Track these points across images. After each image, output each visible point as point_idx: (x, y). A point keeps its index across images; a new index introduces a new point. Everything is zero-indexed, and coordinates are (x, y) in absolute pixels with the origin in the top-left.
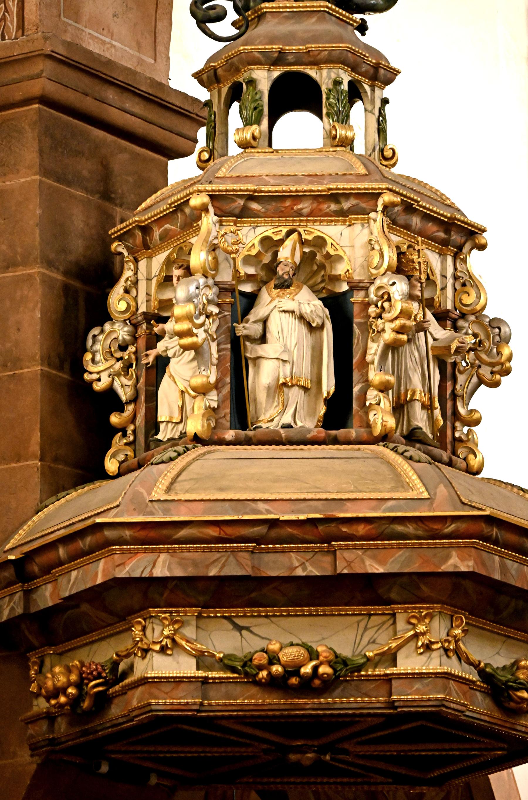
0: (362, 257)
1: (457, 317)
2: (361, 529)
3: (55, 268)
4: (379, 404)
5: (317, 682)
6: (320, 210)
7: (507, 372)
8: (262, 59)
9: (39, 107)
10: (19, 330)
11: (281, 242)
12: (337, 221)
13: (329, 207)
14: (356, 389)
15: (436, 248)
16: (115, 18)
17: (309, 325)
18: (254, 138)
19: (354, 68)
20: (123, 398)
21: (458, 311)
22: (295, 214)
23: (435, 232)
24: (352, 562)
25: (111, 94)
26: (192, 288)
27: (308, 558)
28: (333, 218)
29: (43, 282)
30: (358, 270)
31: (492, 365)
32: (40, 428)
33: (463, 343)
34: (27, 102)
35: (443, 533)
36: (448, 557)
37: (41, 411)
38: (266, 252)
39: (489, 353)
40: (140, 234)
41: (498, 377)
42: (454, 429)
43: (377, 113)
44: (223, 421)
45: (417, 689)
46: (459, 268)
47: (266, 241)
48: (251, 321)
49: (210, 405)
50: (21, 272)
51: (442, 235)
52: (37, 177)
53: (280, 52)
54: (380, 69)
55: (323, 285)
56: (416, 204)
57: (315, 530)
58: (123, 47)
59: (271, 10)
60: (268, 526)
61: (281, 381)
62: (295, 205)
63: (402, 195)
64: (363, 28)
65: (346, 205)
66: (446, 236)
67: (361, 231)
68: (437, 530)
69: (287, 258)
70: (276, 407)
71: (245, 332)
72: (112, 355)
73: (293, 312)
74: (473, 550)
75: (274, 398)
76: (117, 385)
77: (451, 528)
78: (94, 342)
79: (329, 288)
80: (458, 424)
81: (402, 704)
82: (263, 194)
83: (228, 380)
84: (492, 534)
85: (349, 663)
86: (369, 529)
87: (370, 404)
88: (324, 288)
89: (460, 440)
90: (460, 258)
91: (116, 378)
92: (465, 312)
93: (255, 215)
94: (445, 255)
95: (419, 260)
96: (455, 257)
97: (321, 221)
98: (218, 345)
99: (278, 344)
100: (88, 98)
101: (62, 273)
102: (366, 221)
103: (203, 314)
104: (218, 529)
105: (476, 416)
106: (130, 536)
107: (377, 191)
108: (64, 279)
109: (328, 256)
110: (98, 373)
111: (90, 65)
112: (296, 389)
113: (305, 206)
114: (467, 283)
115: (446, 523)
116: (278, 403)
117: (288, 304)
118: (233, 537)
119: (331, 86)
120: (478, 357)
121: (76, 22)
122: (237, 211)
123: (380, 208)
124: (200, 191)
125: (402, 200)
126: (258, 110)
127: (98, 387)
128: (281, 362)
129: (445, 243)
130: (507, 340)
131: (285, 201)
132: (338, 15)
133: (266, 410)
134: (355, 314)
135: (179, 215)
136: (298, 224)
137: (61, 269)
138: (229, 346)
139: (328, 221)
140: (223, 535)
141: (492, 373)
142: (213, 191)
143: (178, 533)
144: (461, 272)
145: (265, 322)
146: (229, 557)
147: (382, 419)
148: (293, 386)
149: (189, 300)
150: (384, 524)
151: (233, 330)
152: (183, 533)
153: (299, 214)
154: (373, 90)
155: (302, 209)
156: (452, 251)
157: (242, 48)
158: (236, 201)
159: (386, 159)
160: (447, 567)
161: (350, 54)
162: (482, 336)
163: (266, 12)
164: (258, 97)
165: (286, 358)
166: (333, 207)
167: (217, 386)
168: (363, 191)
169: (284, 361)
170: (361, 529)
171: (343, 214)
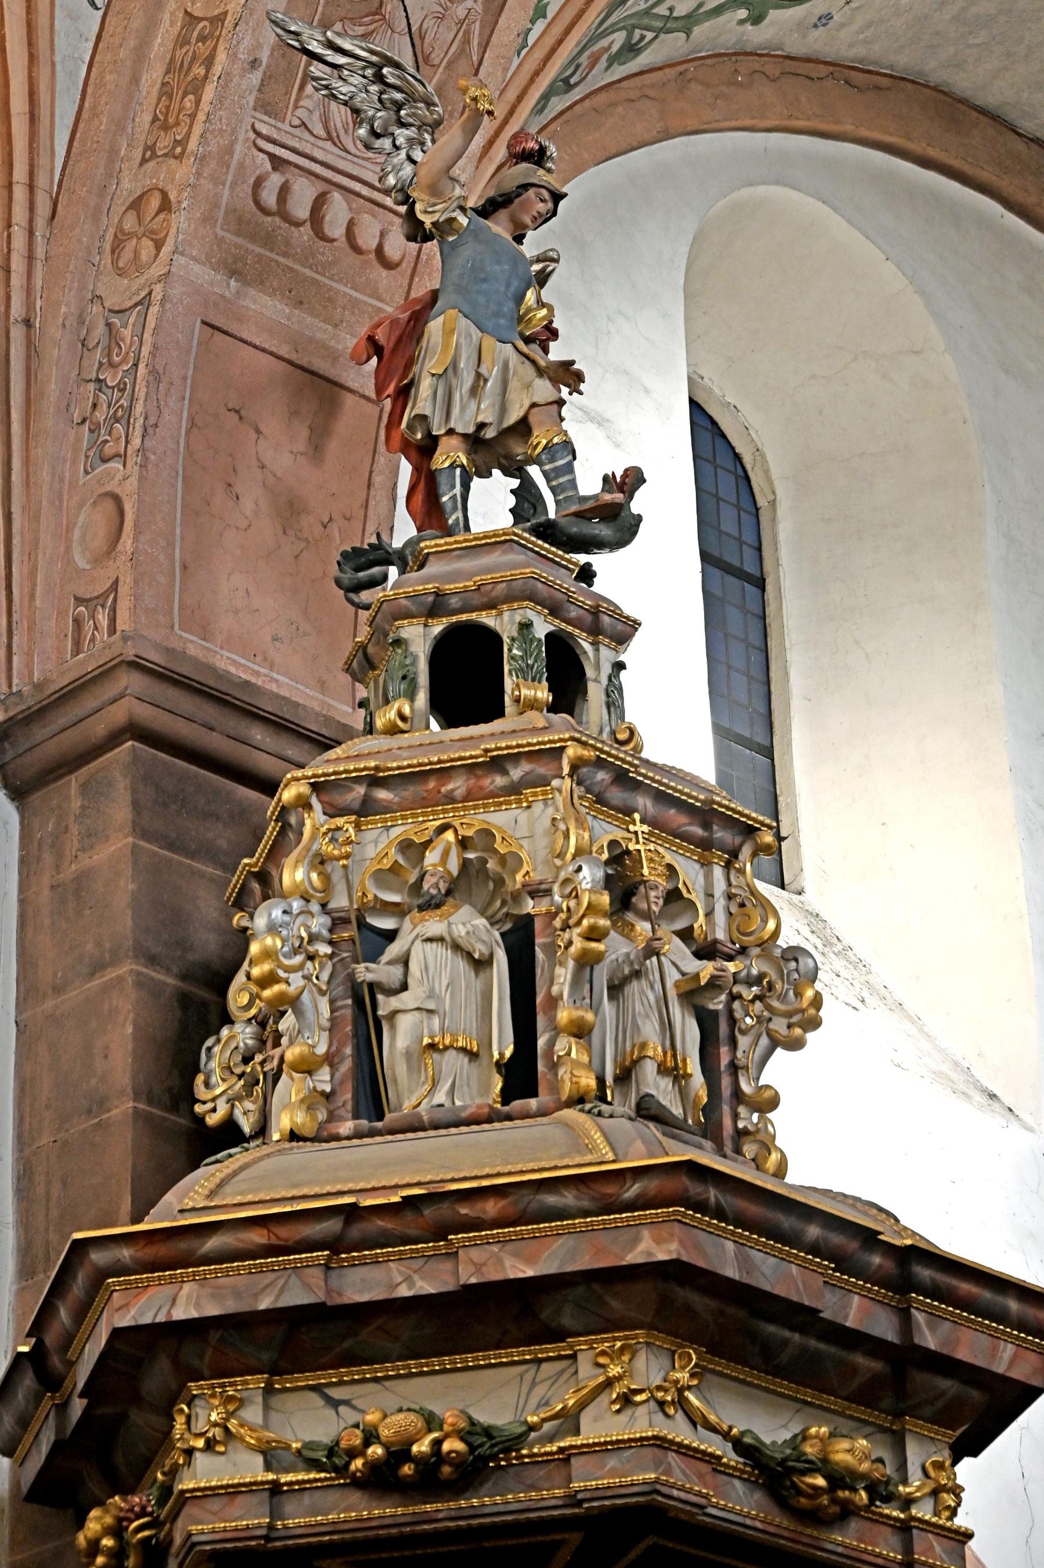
0: (546, 848)
1: (733, 953)
2: (491, 1208)
3: (162, 967)
4: (569, 1054)
5: (446, 1470)
6: (481, 788)
7: (814, 1023)
8: (413, 608)
9: (133, 745)
10: (106, 1057)
11: (427, 844)
12: (509, 803)
13: (493, 782)
14: (541, 1042)
15: (693, 852)
16: (277, 643)
17: (469, 955)
18: (403, 718)
19: (554, 610)
20: (247, 1130)
21: (738, 946)
22: (443, 800)
23: (684, 825)
24: (484, 1264)
25: (258, 734)
26: (277, 913)
27: (416, 1267)
28: (502, 799)
29: (139, 984)
30: (539, 868)
31: (789, 1015)
32: (132, 1190)
33: (723, 971)
34: (114, 739)
35: (622, 1201)
36: (636, 1240)
37: (134, 1167)
38: (414, 868)
39: (782, 998)
40: (257, 886)
41: (798, 1031)
42: (736, 1116)
43: (604, 681)
44: (342, 1112)
45: (612, 1469)
46: (734, 882)
47: (406, 846)
48: (383, 961)
49: (314, 1087)
50: (111, 974)
51: (698, 831)
52: (130, 839)
53: (437, 594)
54: (601, 615)
55: (505, 910)
56: (632, 769)
57: (420, 1219)
58: (290, 682)
59: (434, 550)
60: (342, 1218)
61: (426, 1041)
62: (443, 785)
63: (596, 749)
64: (586, 574)
65: (516, 773)
66: (706, 834)
67: (543, 811)
68: (611, 1196)
69: (434, 865)
70: (424, 1083)
71: (370, 977)
72: (232, 1073)
73: (441, 939)
74: (676, 1223)
75: (420, 1071)
76: (238, 1114)
77: (633, 1190)
78: (209, 1057)
79: (515, 912)
80: (742, 1110)
81: (588, 1495)
82: (391, 773)
83: (348, 1051)
84: (708, 1198)
85: (495, 1434)
86: (503, 1207)
87: (559, 1057)
88: (507, 914)
89: (745, 1133)
90: (735, 868)
91: (237, 1103)
92: (747, 945)
93: (386, 809)
94: (711, 863)
95: (638, 847)
96: (728, 866)
97: (485, 806)
98: (332, 1002)
99: (421, 989)
100: (215, 734)
101: (177, 975)
102: (550, 796)
103: (301, 953)
104: (265, 1232)
105: (768, 1094)
106: (131, 1257)
107: (558, 745)
108: (179, 983)
109: (503, 860)
110: (214, 1100)
111: (211, 683)
113: (457, 785)
114: (747, 903)
115: (625, 1183)
116: (427, 1078)
117: (434, 926)
118: (290, 1243)
119: (515, 634)
120: (769, 1008)
121: (204, 640)
122: (356, 805)
123: (566, 770)
124: (298, 779)
125: (598, 756)
126: (408, 679)
127: (212, 1120)
128: (424, 1013)
129: (705, 845)
130: (813, 978)
131: (426, 782)
132: (537, 549)
133: (411, 1092)
134: (537, 932)
135: (290, 835)
136: (451, 815)
137: (175, 970)
138: (349, 1002)
139: (495, 804)
140: (274, 1241)
141: (789, 1026)
142: (314, 776)
143: (203, 1244)
144: (736, 887)
145: (405, 961)
146: (289, 1276)
147: (571, 1073)
148: (446, 1048)
149: (273, 929)
150: (523, 1196)
151: (351, 977)
152: (213, 1243)
153: (450, 799)
154: (597, 650)
155: (453, 790)
156: (720, 857)
157: (381, 595)
158: (351, 790)
159: (622, 743)
160: (634, 1257)
161: (540, 585)
162: (773, 975)
163: (428, 554)
164: (408, 661)
165: (431, 1005)
166: (500, 781)
167: (330, 1059)
168: (537, 748)
169: (430, 1012)
170: (491, 1208)
171: (514, 790)
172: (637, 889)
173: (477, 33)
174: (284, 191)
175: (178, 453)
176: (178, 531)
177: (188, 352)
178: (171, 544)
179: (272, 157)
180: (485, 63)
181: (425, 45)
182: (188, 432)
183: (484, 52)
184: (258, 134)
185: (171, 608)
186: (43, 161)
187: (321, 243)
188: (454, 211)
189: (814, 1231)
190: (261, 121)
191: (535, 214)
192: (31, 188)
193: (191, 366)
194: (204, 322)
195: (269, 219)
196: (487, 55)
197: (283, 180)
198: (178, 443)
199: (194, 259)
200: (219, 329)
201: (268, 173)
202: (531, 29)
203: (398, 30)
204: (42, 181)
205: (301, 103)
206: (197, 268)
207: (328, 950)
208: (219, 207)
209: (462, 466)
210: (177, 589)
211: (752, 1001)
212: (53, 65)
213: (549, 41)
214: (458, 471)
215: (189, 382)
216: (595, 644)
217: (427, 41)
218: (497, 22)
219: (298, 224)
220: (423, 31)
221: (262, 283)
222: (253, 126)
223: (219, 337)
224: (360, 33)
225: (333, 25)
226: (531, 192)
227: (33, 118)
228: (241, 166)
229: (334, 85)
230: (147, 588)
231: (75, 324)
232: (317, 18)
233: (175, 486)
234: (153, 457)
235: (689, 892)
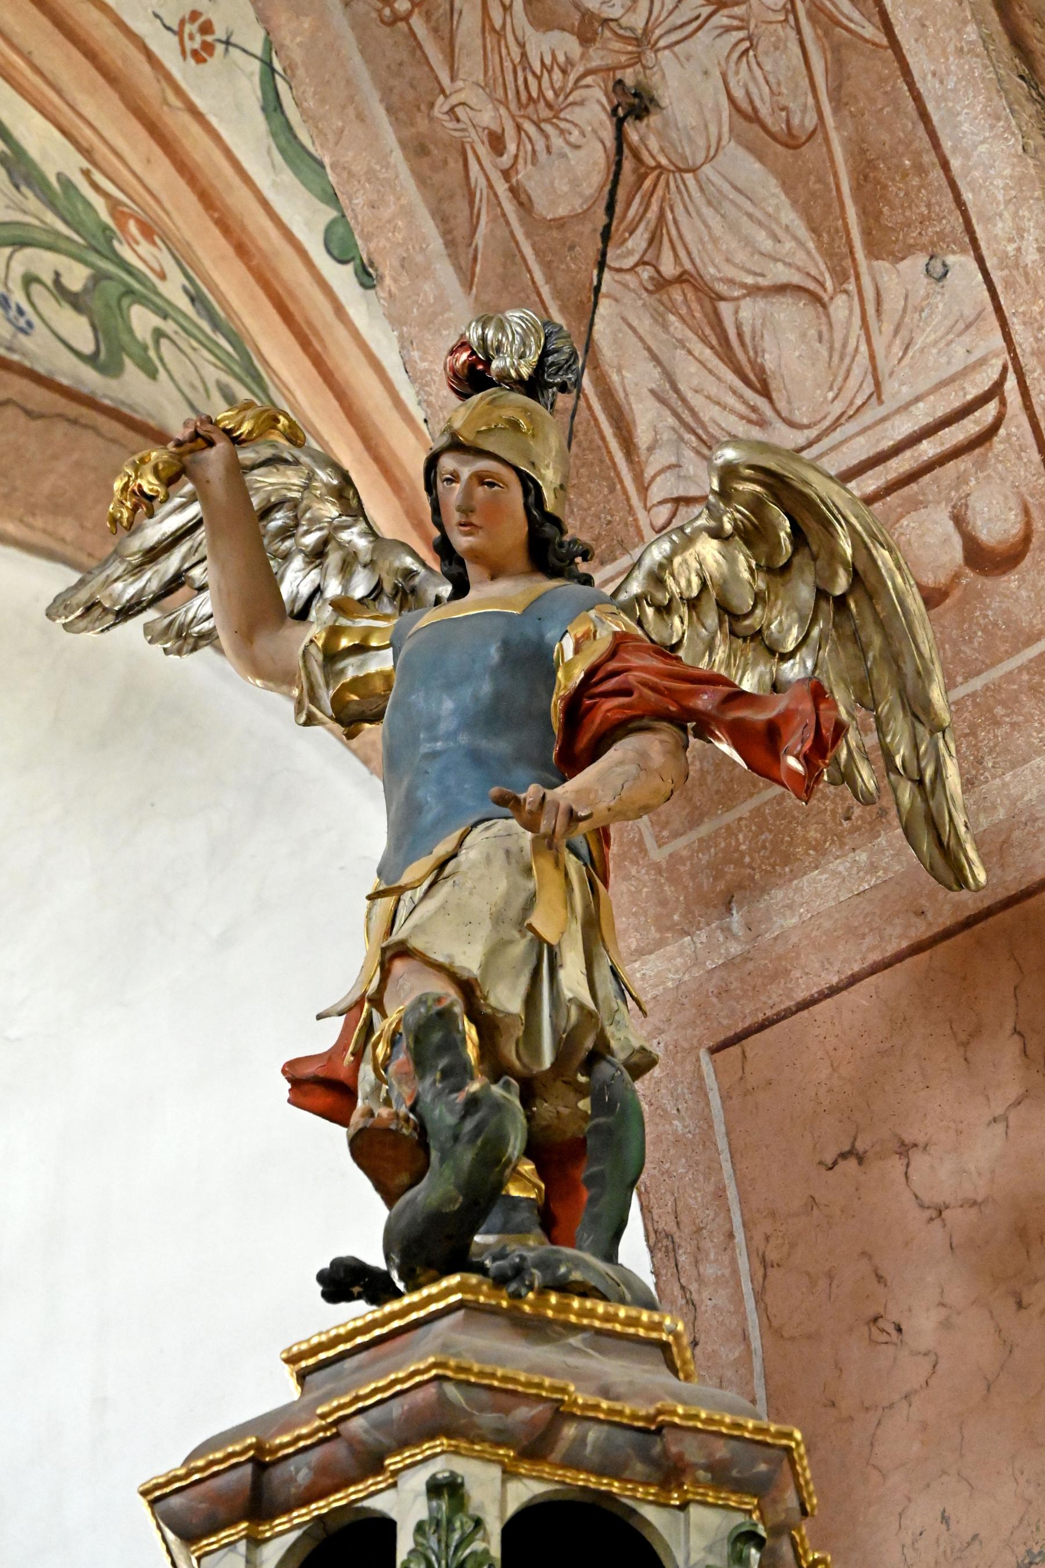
181: (769, 121)
203: (701, 157)
205: (649, 472)
215: (732, 1193)
217: (764, 111)
220: (745, 105)
221: (787, 859)
224: (644, 245)
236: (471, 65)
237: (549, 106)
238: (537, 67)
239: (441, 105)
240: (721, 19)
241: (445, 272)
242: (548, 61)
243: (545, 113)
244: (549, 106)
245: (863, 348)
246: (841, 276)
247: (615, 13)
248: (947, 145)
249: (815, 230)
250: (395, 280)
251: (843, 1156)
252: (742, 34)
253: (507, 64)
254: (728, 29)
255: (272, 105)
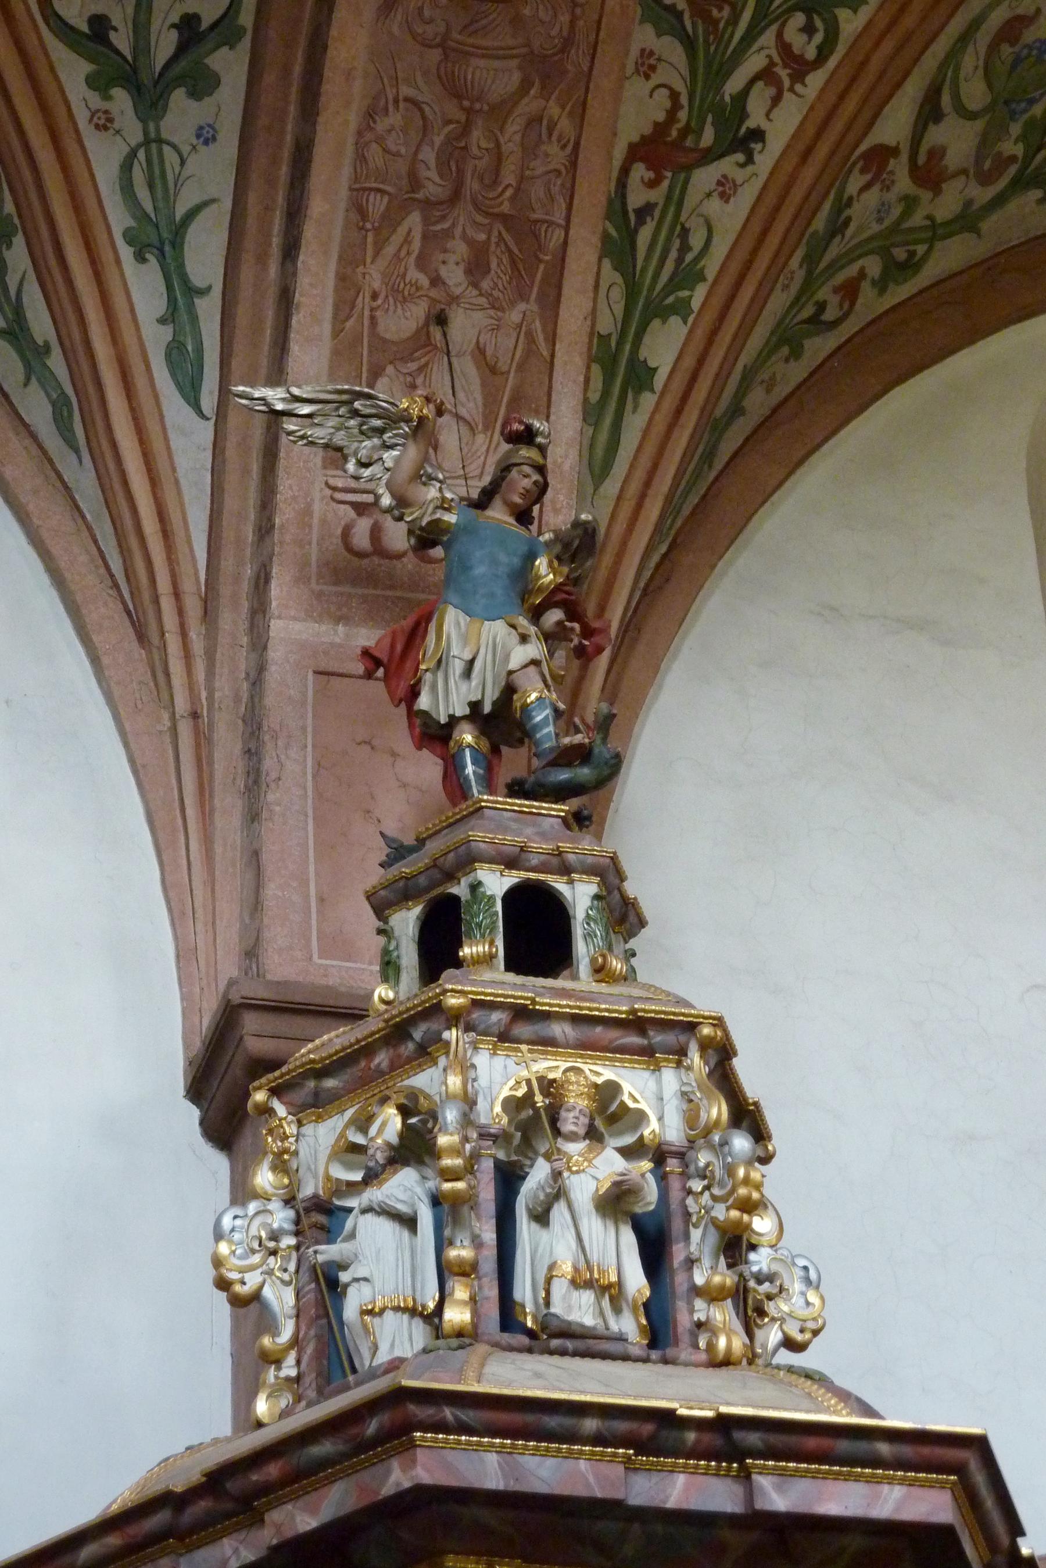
8: (392, 896)
23: (617, 1039)
27: (242, 1538)
36: (388, 1473)
54: (564, 854)
66: (646, 1042)
84: (445, 1417)
112: (389, 1315)
113: (382, 1059)
121: (349, 959)
148: (382, 1311)
155: (379, 1064)
160: (388, 1489)
172: (558, 1113)
173: (539, 330)
174: (376, 532)
175: (305, 796)
176: (312, 868)
177: (304, 703)
178: (306, 883)
179: (355, 505)
180: (559, 354)
181: (488, 358)
182: (314, 777)
183: (554, 345)
184: (334, 489)
185: (308, 940)
186: (185, 568)
187: (429, 566)
188: (434, 512)
189: (590, 1425)
190: (335, 476)
191: (522, 491)
192: (177, 595)
193: (310, 715)
194: (317, 673)
195: (366, 561)
196: (558, 346)
197: (372, 521)
198: (305, 788)
199: (295, 619)
200: (333, 674)
201: (353, 521)
202: (691, 297)
204: (187, 586)
206: (298, 626)
207: (292, 1241)
208: (310, 565)
209: (469, 746)
210: (314, 922)
211: (702, 1193)
212: (177, 482)
213: (717, 302)
214: (468, 752)
216: (571, 882)
218: (557, 315)
219: (400, 556)
220: (481, 346)
222: (327, 484)
223: (335, 681)
225: (384, 369)
226: (514, 473)
227: (166, 534)
228: (324, 522)
229: (309, 433)
230: (279, 929)
231: (232, 704)
232: (364, 369)
233: (305, 829)
234: (277, 808)
235: (635, 1100)
236: (382, 263)
237: (404, 297)
238: (407, 281)
239: (361, 269)
240: (492, 312)
241: (327, 328)
242: (413, 281)
243: (400, 298)
244: (404, 297)
245: (482, 458)
246: (486, 428)
247: (451, 283)
248: (553, 410)
249: (485, 405)
250: (304, 317)
251: (365, 742)
252: (494, 322)
253: (396, 273)
254: (492, 318)
255: (127, 167)
